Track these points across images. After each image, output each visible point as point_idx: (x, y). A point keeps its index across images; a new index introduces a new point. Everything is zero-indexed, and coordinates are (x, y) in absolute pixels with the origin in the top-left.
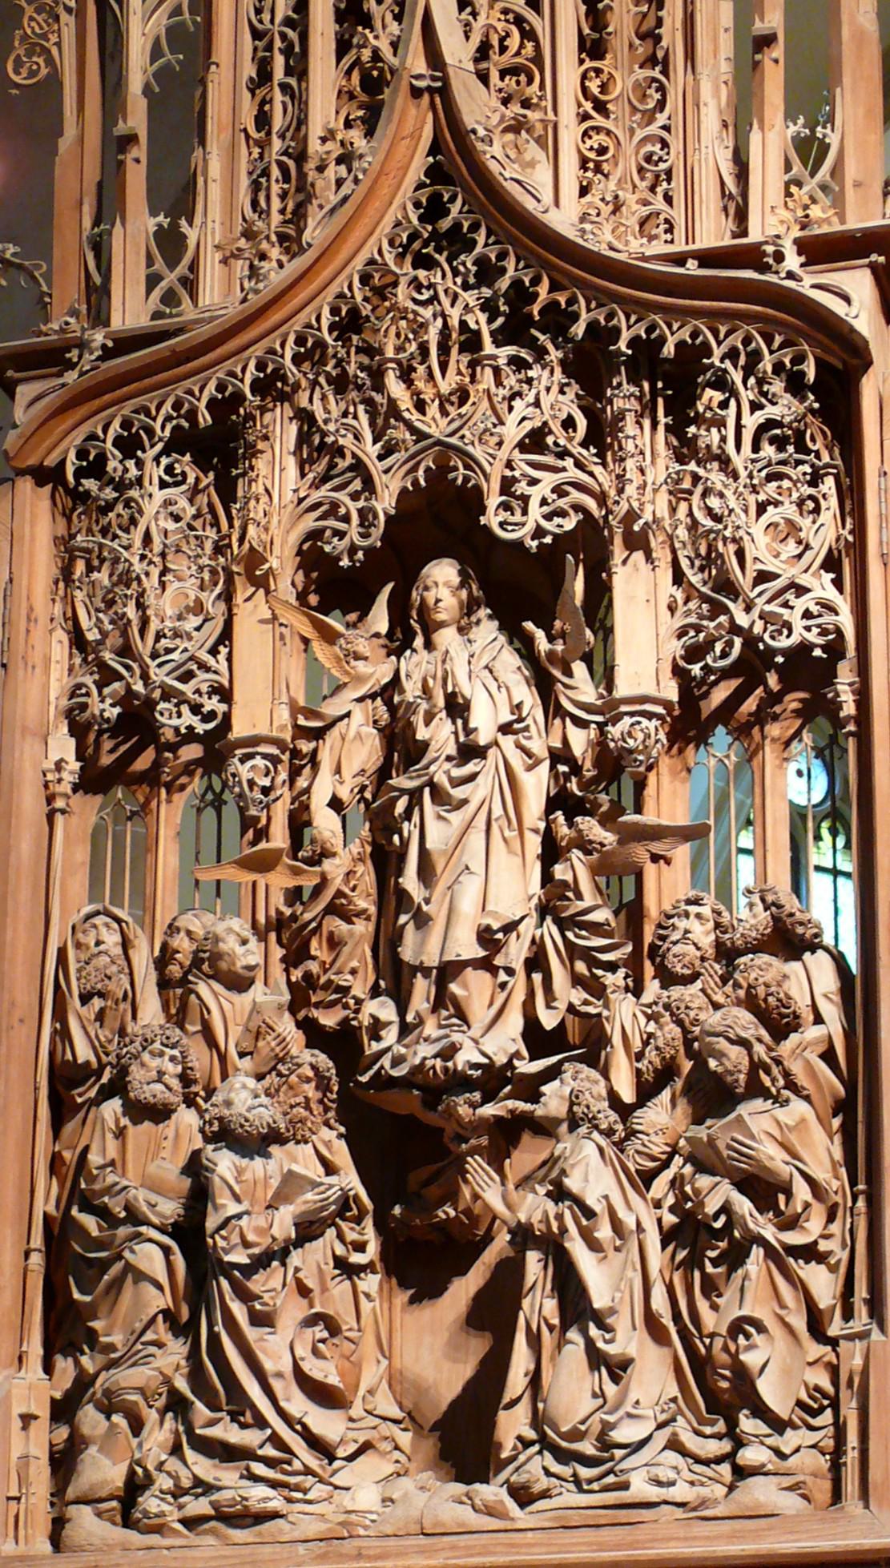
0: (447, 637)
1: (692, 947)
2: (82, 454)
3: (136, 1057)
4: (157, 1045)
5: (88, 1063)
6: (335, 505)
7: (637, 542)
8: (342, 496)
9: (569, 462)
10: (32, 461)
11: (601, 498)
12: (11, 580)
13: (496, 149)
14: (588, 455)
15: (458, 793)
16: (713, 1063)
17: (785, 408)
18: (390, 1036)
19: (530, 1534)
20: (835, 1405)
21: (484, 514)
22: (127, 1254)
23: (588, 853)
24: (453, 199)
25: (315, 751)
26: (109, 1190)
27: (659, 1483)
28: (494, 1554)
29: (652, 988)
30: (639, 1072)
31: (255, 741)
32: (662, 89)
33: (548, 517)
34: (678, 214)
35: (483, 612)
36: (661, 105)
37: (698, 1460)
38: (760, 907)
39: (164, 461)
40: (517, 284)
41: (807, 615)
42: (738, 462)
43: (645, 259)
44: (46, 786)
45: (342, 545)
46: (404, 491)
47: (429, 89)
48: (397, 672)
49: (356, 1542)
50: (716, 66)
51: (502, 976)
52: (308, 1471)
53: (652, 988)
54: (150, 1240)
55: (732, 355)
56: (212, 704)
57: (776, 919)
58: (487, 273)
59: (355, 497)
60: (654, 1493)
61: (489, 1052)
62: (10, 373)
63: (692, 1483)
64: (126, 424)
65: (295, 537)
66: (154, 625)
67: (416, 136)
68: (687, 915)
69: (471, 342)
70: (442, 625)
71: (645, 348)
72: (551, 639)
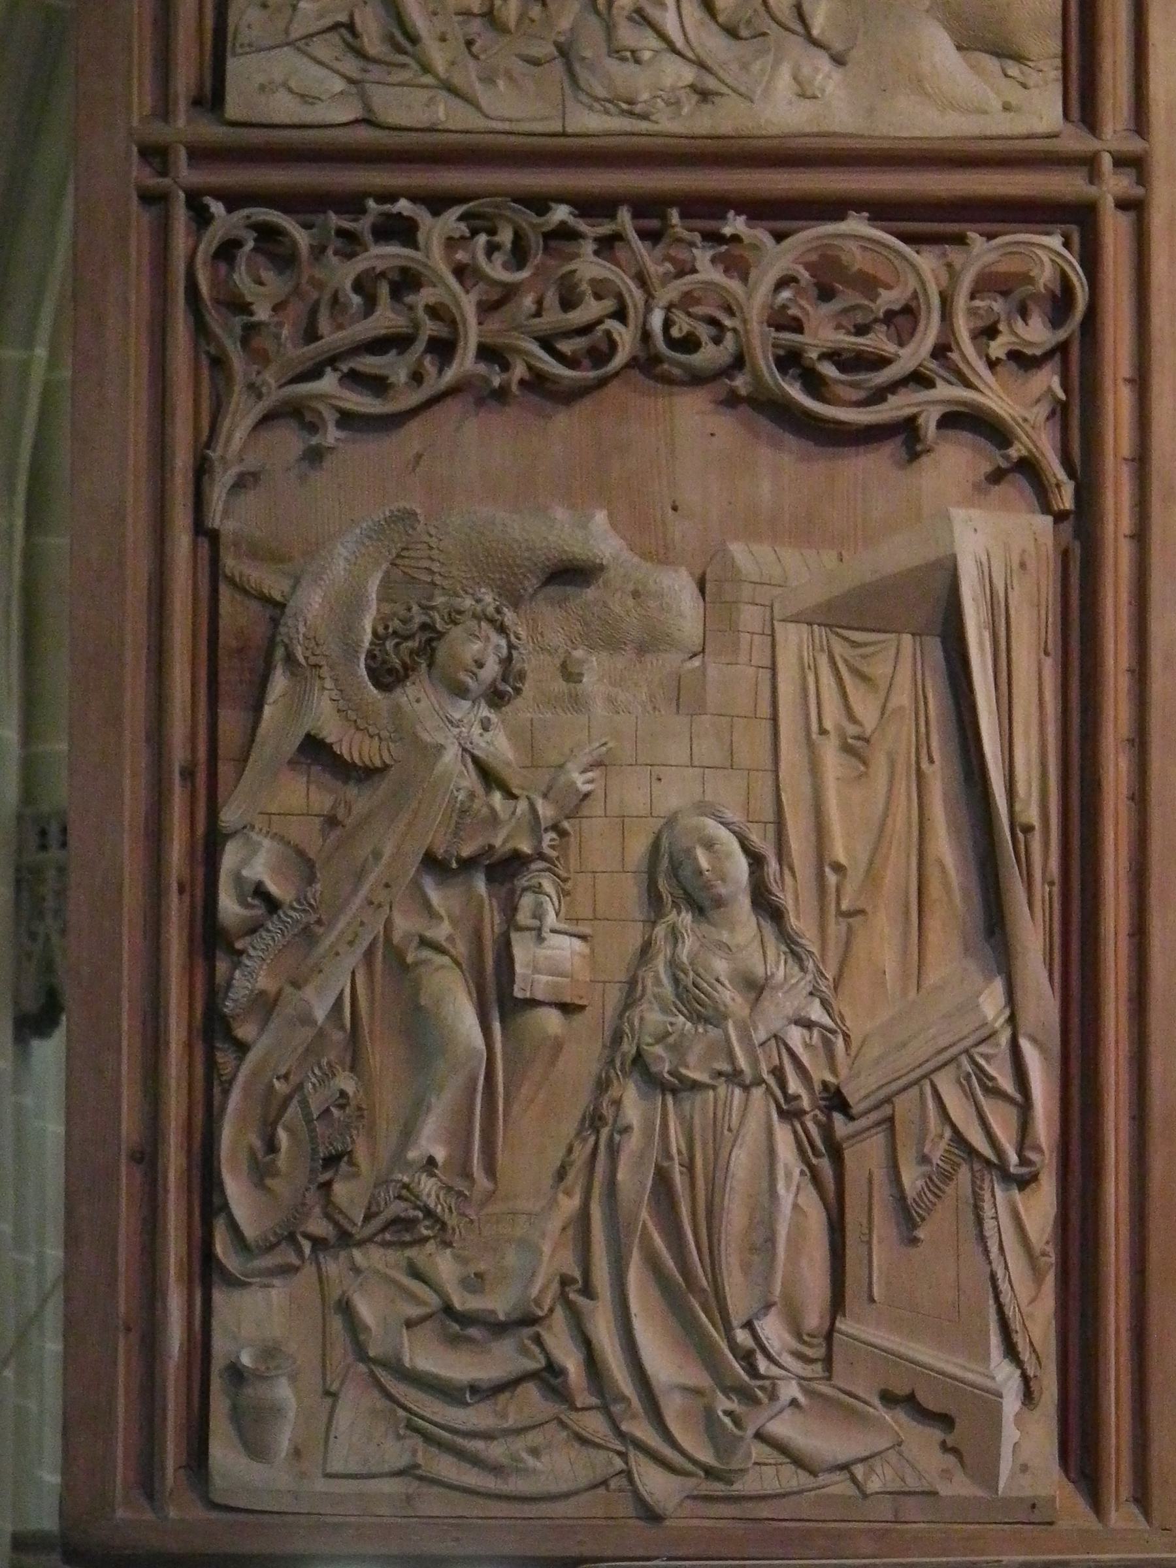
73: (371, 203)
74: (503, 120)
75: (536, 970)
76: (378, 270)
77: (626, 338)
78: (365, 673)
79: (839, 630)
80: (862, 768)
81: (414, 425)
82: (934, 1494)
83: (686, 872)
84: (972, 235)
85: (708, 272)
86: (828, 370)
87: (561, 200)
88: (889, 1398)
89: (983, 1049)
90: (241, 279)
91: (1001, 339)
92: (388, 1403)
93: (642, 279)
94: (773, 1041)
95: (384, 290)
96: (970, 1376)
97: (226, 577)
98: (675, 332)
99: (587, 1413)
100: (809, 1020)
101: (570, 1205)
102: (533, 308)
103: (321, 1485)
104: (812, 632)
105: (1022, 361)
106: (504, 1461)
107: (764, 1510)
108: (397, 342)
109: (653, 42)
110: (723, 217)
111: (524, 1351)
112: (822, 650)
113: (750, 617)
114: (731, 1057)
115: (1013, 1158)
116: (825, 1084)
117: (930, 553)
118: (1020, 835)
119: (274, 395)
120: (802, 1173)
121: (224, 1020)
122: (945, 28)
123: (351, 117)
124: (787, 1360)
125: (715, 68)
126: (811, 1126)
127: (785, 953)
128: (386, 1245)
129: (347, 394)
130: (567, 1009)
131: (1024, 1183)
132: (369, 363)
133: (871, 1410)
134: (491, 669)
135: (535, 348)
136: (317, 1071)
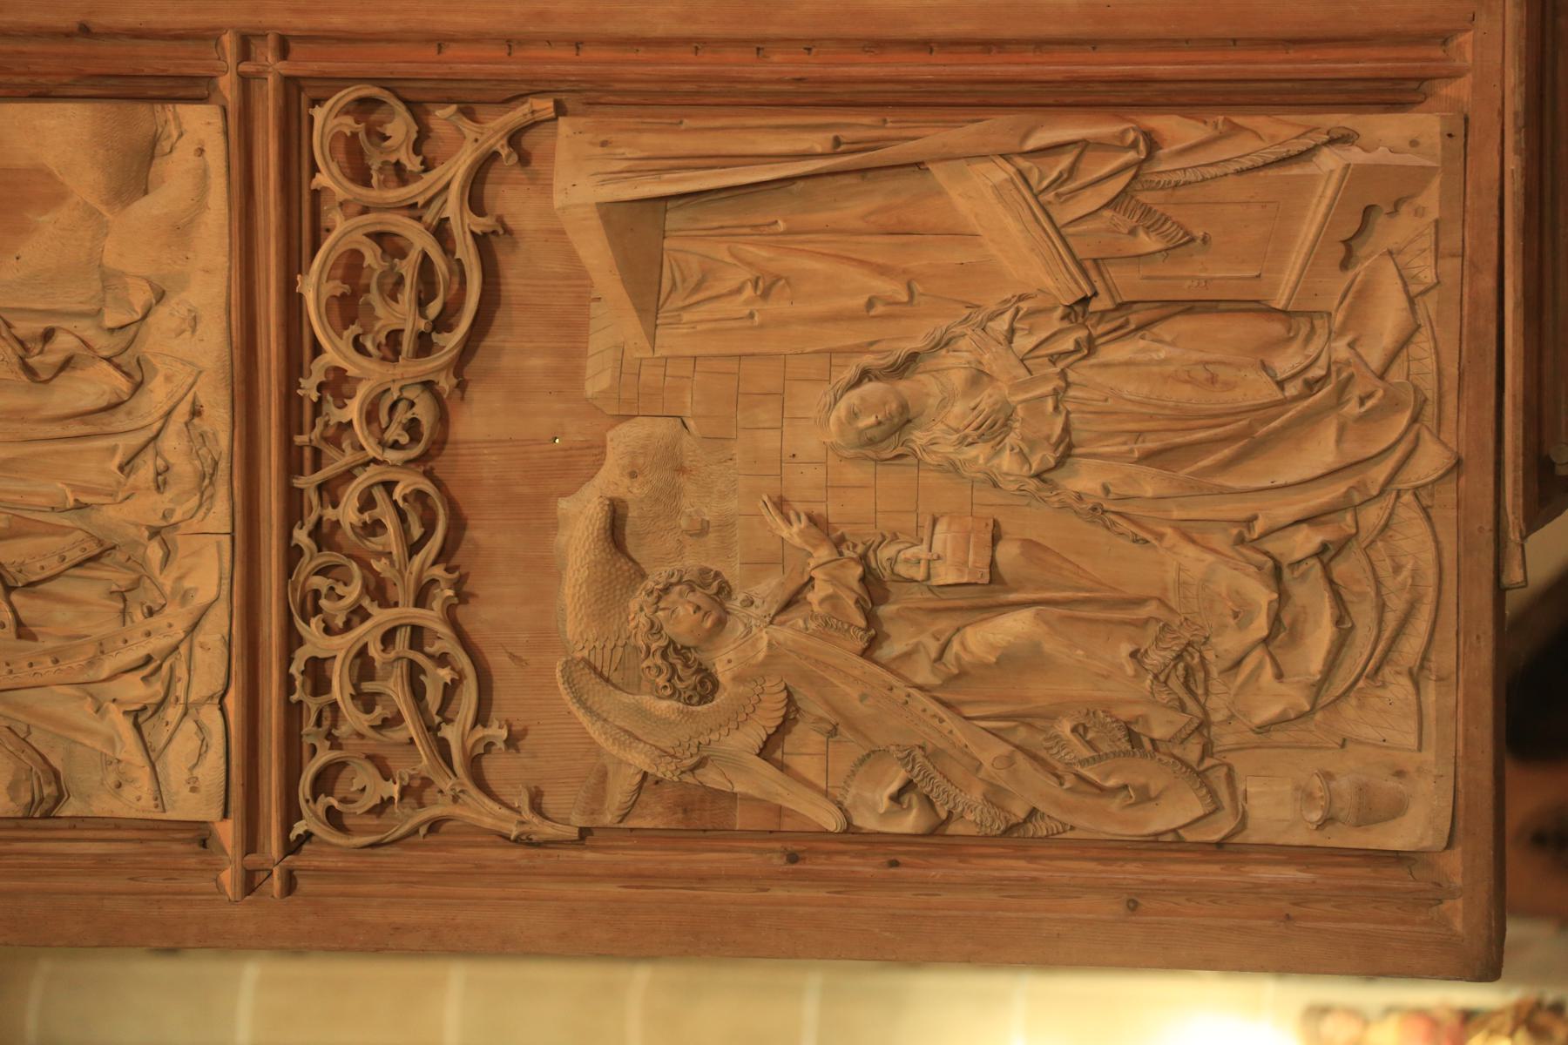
73: (294, 698)
74: (220, 585)
75: (965, 563)
76: (353, 693)
78: (705, 706)
79: (661, 302)
80: (782, 282)
82: (1437, 222)
83: (876, 432)
84: (315, 183)
85: (353, 411)
86: (434, 309)
87: (289, 536)
88: (1345, 265)
89: (1034, 180)
90: (360, 807)
91: (404, 160)
92: (1352, 694)
94: (1026, 362)
95: (368, 687)
96: (1329, 192)
97: (620, 822)
98: (404, 439)
99: (1361, 524)
100: (1007, 331)
102: (384, 560)
103: (1429, 755)
104: (662, 324)
106: (1406, 596)
107: (1452, 371)
108: (414, 674)
109: (149, 455)
110: (301, 399)
111: (1304, 576)
112: (679, 315)
114: (1043, 397)
115: (1131, 156)
116: (1063, 318)
117: (596, 222)
118: (843, 148)
120: (1143, 338)
121: (1010, 829)
122: (128, 204)
123: (218, 713)
124: (1312, 350)
125: (171, 403)
126: (1101, 329)
127: (948, 351)
128: (1207, 692)
129: (460, 717)
130: (996, 539)
131: (1152, 143)
132: (433, 698)
133: (1359, 278)
135: (417, 559)
136: (1055, 751)
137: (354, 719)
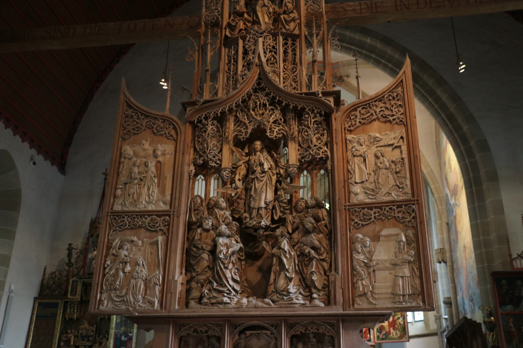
0: (258, 153)
1: (302, 207)
2: (198, 119)
3: (204, 221)
4: (208, 219)
5: (195, 222)
6: (240, 131)
7: (293, 139)
8: (242, 129)
9: (281, 126)
10: (190, 120)
11: (286, 132)
12: (185, 139)
13: (270, 75)
14: (284, 125)
15: (262, 179)
16: (307, 227)
17: (319, 119)
18: (248, 220)
19: (275, 309)
20: (328, 287)
21: (266, 132)
22: (202, 255)
23: (284, 190)
24: (262, 82)
25: (235, 171)
26: (199, 244)
27: (298, 300)
28: (268, 312)
29: (294, 214)
30: (292, 228)
31: (226, 168)
32: (296, 68)
33: (277, 134)
34: (299, 88)
35: (265, 150)
36: (296, 71)
37: (305, 296)
38: (314, 200)
39: (212, 121)
40: (273, 97)
41: (322, 152)
42: (311, 127)
43: (296, 93)
44: (189, 174)
45: (242, 137)
46: (253, 129)
47: (259, 65)
48: (249, 159)
49: (243, 309)
50: (305, 66)
51: (268, 210)
52: (234, 296)
53: (294, 214)
54: (206, 253)
55: (309, 110)
56: (218, 162)
57: (316, 202)
58: (267, 95)
59: (244, 129)
60: (297, 302)
61: (267, 223)
62: (186, 106)
63: (304, 300)
64: (206, 115)
65: (233, 135)
66: (209, 148)
67: (256, 72)
68: (301, 201)
69: (265, 105)
70: (258, 151)
71: (295, 108)
72: (277, 154)
77: (138, 224)
81: (124, 232)
85: (144, 220)
93: (140, 221)
101: (127, 287)
103: (107, 309)
105: (165, 226)
113: (145, 244)
119: (114, 229)
134: (126, 248)
137: (119, 221)
